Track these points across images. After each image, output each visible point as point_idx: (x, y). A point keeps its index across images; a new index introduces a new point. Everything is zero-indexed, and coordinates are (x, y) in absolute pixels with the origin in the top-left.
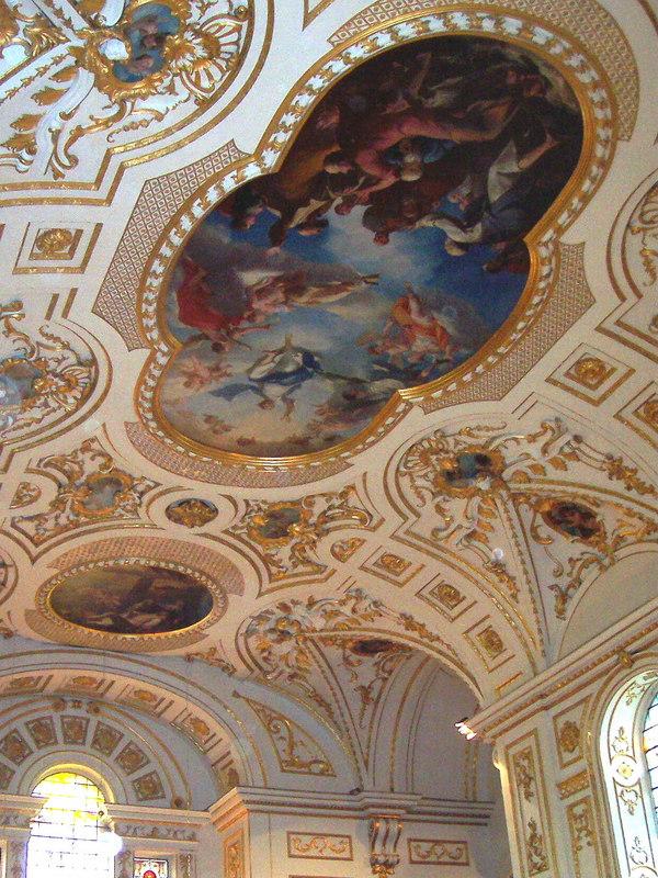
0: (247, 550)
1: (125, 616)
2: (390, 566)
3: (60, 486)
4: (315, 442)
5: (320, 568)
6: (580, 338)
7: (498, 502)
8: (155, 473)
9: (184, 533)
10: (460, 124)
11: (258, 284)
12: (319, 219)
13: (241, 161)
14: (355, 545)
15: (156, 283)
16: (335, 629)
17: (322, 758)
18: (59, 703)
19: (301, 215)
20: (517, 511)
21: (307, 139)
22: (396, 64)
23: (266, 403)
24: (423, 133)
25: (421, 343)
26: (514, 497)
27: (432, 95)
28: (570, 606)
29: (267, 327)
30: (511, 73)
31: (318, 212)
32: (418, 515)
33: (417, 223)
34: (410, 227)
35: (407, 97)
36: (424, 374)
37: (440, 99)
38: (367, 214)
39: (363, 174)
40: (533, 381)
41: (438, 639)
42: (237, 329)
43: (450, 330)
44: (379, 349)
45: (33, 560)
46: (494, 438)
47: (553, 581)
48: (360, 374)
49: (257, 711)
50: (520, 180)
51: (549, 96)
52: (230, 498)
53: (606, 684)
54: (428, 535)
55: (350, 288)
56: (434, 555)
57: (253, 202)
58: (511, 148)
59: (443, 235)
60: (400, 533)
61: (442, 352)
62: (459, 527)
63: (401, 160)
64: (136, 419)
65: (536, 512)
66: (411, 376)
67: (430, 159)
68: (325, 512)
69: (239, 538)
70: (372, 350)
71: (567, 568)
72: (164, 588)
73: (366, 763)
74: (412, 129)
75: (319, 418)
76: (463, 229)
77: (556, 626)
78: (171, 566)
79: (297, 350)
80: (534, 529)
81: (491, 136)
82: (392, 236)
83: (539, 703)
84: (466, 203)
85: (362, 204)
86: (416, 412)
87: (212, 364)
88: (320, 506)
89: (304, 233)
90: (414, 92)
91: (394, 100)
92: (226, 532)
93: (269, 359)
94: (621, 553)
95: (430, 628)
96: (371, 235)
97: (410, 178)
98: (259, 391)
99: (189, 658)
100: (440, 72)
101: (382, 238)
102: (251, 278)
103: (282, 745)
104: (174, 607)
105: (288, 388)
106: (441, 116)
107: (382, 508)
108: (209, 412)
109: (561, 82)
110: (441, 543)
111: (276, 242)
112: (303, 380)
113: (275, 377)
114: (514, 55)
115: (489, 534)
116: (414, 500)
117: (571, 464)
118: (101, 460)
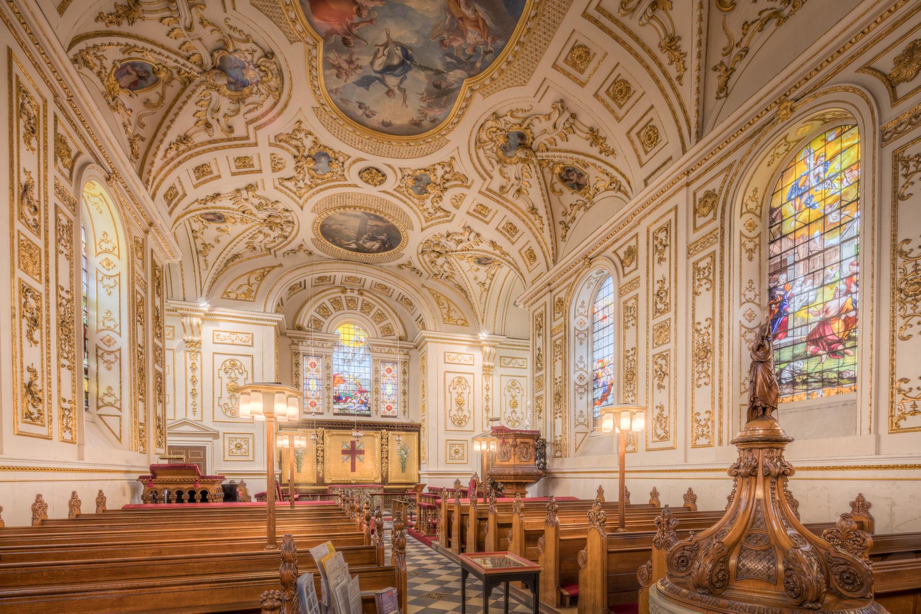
0: (407, 200)
1: (361, 242)
2: (481, 212)
4: (426, 123)
7: (532, 166)
17: (463, 318)
18: (344, 291)
20: (542, 172)
23: (390, 92)
29: (371, 21)
32: (491, 178)
36: (478, 65)
40: (544, 68)
41: (508, 254)
43: (488, 22)
46: (526, 118)
48: (439, 66)
49: (433, 295)
52: (389, 166)
54: (497, 190)
56: (502, 204)
60: (484, 190)
62: (513, 185)
64: (317, 105)
65: (553, 173)
66: (472, 71)
68: (443, 177)
72: (374, 226)
73: (483, 320)
78: (373, 212)
79: (397, 44)
80: (552, 185)
86: (478, 96)
87: (346, 57)
88: (440, 172)
92: (394, 190)
93: (380, 54)
95: (504, 249)
98: (382, 81)
99: (400, 266)
103: (445, 311)
104: (383, 237)
105: (400, 78)
107: (472, 175)
108: (362, 100)
110: (505, 196)
112: (406, 72)
113: (388, 69)
115: (529, 189)
116: (489, 168)
117: (571, 136)
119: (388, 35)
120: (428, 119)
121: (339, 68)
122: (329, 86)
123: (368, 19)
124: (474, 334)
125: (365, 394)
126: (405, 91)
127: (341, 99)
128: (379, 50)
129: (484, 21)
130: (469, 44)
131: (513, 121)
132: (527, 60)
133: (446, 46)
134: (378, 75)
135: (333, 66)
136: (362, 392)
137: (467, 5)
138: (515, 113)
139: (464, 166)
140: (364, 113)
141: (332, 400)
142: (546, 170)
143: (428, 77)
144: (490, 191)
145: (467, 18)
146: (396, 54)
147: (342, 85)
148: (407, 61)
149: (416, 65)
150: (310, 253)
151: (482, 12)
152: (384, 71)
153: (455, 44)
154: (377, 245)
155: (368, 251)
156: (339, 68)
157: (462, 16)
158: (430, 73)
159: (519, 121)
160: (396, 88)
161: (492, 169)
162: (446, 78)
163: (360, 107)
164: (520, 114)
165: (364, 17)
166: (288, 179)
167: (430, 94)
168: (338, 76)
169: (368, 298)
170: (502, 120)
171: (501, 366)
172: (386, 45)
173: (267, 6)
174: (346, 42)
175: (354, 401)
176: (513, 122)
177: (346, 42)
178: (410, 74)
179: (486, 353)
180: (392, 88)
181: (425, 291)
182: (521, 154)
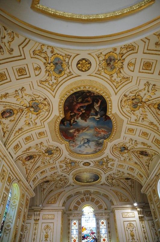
3: (65, 164)
5: (111, 168)
6: (125, 126)
8: (78, 160)
9: (86, 167)
10: (85, 103)
13: (58, 117)
14: (114, 164)
15: (58, 135)
16: (119, 177)
19: (72, 121)
21: (66, 112)
23: (86, 147)
25: (102, 133)
26: (132, 152)
28: (150, 167)
31: (74, 120)
35: (75, 102)
37: (80, 101)
45: (69, 175)
47: (146, 164)
50: (100, 107)
51: (95, 94)
52: (91, 161)
53: (156, 182)
57: (64, 121)
58: (95, 103)
69: (96, 166)
70: (96, 136)
71: (147, 162)
74: (79, 106)
75: (96, 147)
76: (97, 116)
77: (149, 171)
79: (85, 139)
80: (139, 156)
81: (91, 102)
82: (87, 120)
83: (149, 186)
91: (74, 103)
94: (153, 158)
98: (84, 145)
99: (102, 185)
100: (77, 97)
101: (86, 121)
102: (71, 131)
106: (81, 102)
107: (114, 158)
111: (71, 126)
113: (85, 143)
114: (86, 91)
116: (119, 156)
118: (69, 160)
124: (132, 204)
125: (94, 234)
136: (93, 233)
139: (111, 157)
141: (81, 238)
142: (135, 153)
145: (100, 131)
148: (88, 141)
150: (73, 186)
151: (103, 129)
153: (99, 136)
154: (93, 180)
155: (91, 182)
166: (64, 169)
167: (96, 145)
169: (93, 196)
171: (147, 216)
172: (83, 139)
175: (90, 238)
179: (138, 211)
181: (112, 191)
182: (126, 151)
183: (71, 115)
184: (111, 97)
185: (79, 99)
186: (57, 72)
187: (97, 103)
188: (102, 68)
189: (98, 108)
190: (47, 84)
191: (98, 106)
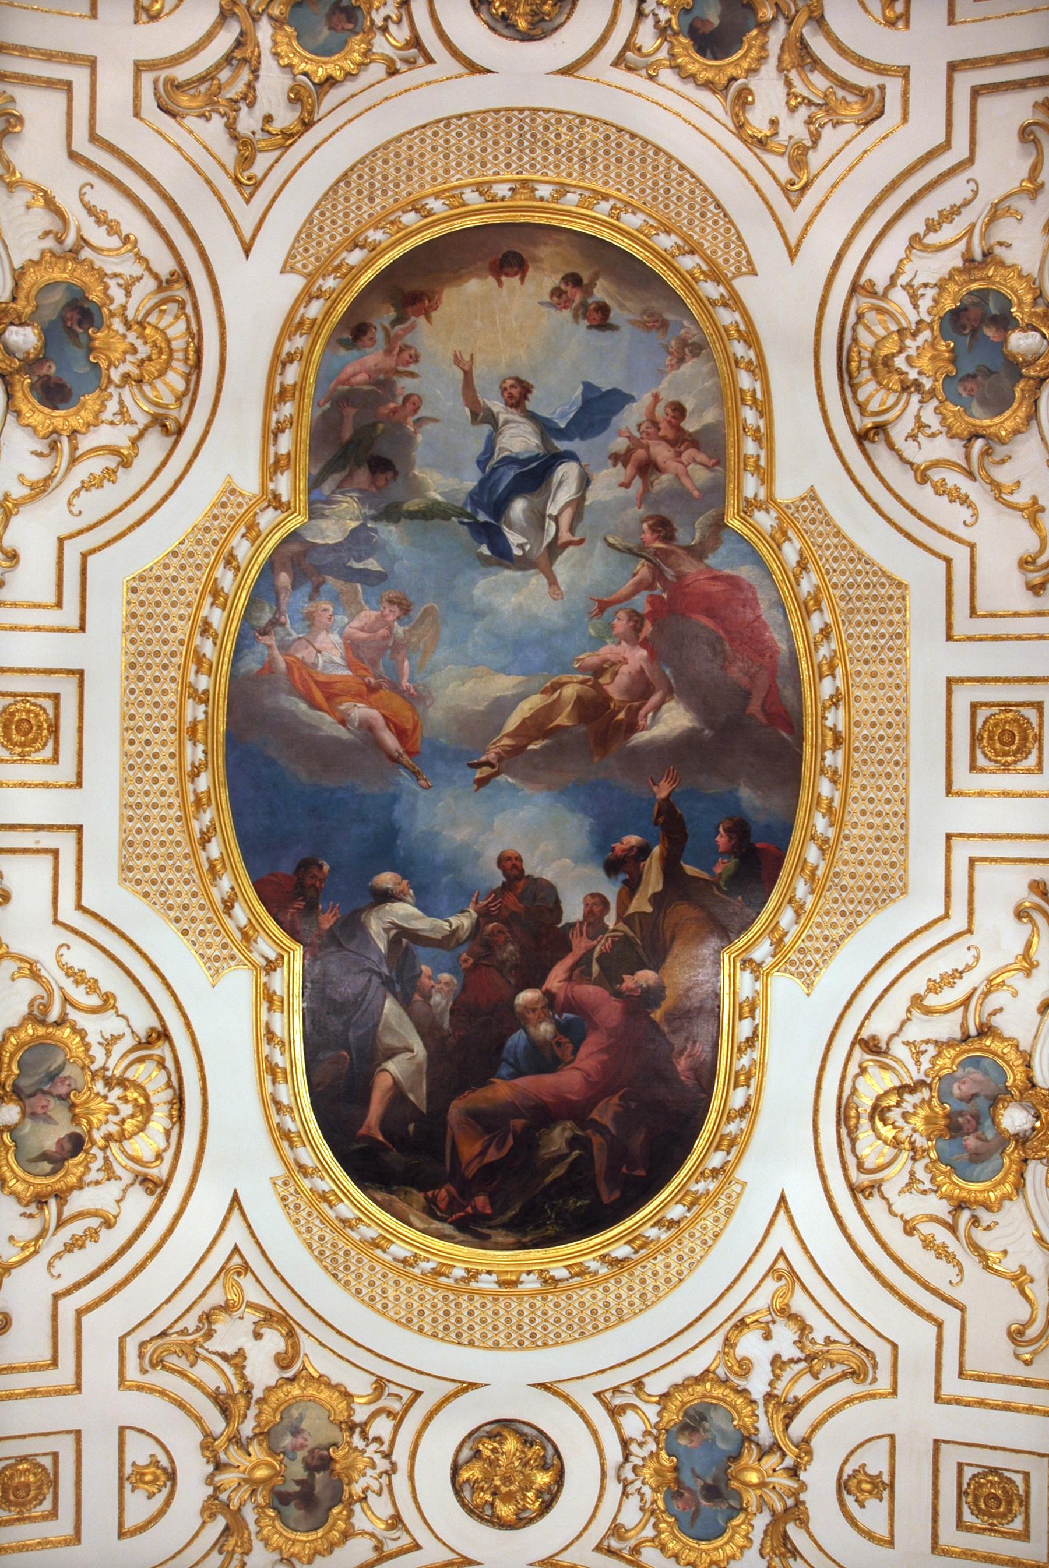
10: (511, 1110)
11: (657, 708)
12: (622, 877)
19: (653, 880)
22: (641, 1172)
24: (549, 1079)
27: (573, 1142)
29: (603, 606)
30: (489, 1211)
31: (632, 887)
33: (475, 915)
34: (483, 903)
37: (558, 1138)
38: (557, 909)
39: (598, 982)
42: (651, 586)
43: (303, 706)
44: (392, 613)
48: (389, 533)
51: (419, 1197)
55: (507, 741)
58: (419, 1097)
59: (427, 911)
61: (284, 647)
63: (557, 1024)
67: (518, 1038)
79: (525, 563)
82: (499, 879)
84: (425, 980)
85: (571, 926)
87: (662, 482)
89: (633, 840)
90: (597, 1140)
91: (617, 1118)
93: (565, 520)
96: (532, 867)
97: (527, 996)
98: (546, 428)
105: (496, 458)
109: (413, 1219)
112: (482, 483)
114: (499, 1236)
119: (553, 581)
120: (380, 336)
121: (680, 440)
122: (705, 369)
123: (610, 610)
126: (474, 415)
127: (664, 325)
128: (572, 529)
129: (314, 705)
130: (328, 630)
131: (104, 435)
132: (157, 654)
133: (391, 602)
134: (562, 445)
135: (694, 441)
137: (367, 727)
138: (112, 462)
140: (588, 291)
143: (416, 488)
144: (50, 84)
145: (359, 697)
146: (523, 535)
147: (664, 384)
149: (460, 513)
151: (327, 724)
152: (551, 461)
156: (680, 440)
157: (374, 696)
158: (413, 504)
159: (85, 443)
160: (502, 418)
161: (91, 197)
162: (362, 501)
163: (603, 309)
164: (77, 1228)
165: (622, 614)
168: (679, 410)
170: (142, 420)
172: (555, 549)
173: (867, 586)
174: (663, 527)
176: (105, 428)
177: (663, 527)
178: (471, 479)
180: (515, 416)
183: (656, 969)
184: (278, 1170)
185: (560, 1158)
186: (717, 1420)
187: (398, 1094)
188: (364, 1436)
189: (389, 1040)
190: (821, 1329)
191: (391, 1066)
